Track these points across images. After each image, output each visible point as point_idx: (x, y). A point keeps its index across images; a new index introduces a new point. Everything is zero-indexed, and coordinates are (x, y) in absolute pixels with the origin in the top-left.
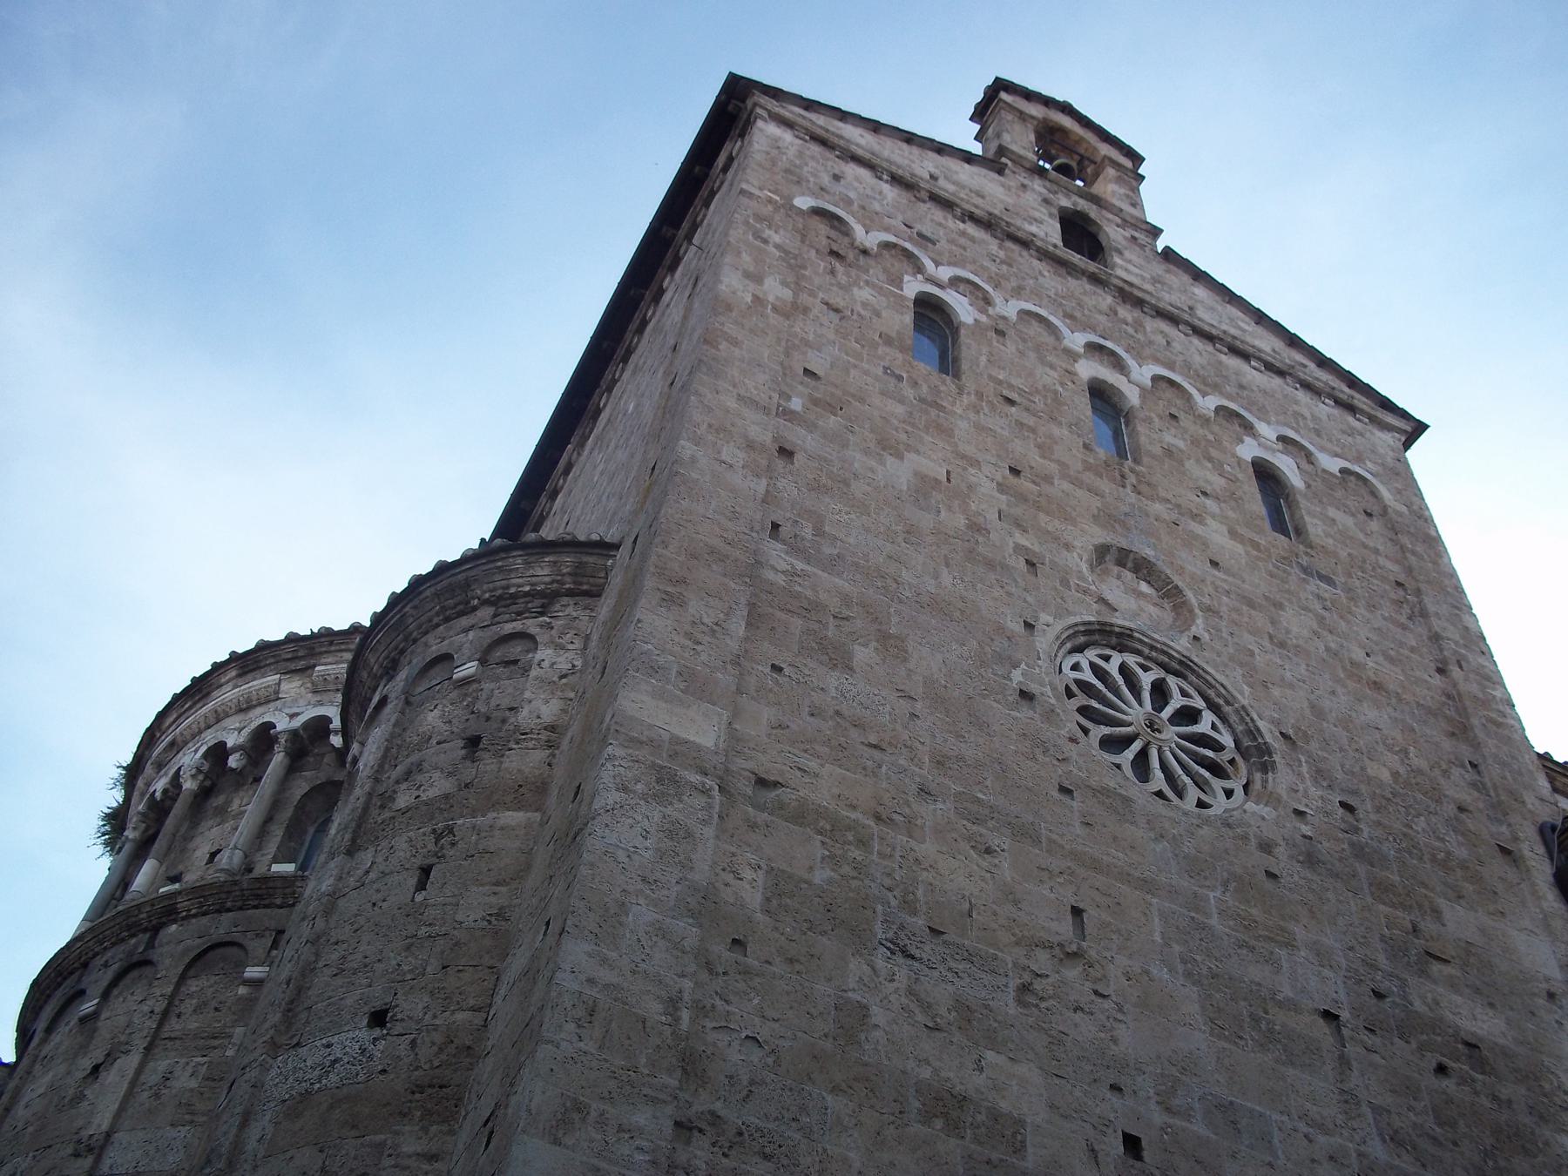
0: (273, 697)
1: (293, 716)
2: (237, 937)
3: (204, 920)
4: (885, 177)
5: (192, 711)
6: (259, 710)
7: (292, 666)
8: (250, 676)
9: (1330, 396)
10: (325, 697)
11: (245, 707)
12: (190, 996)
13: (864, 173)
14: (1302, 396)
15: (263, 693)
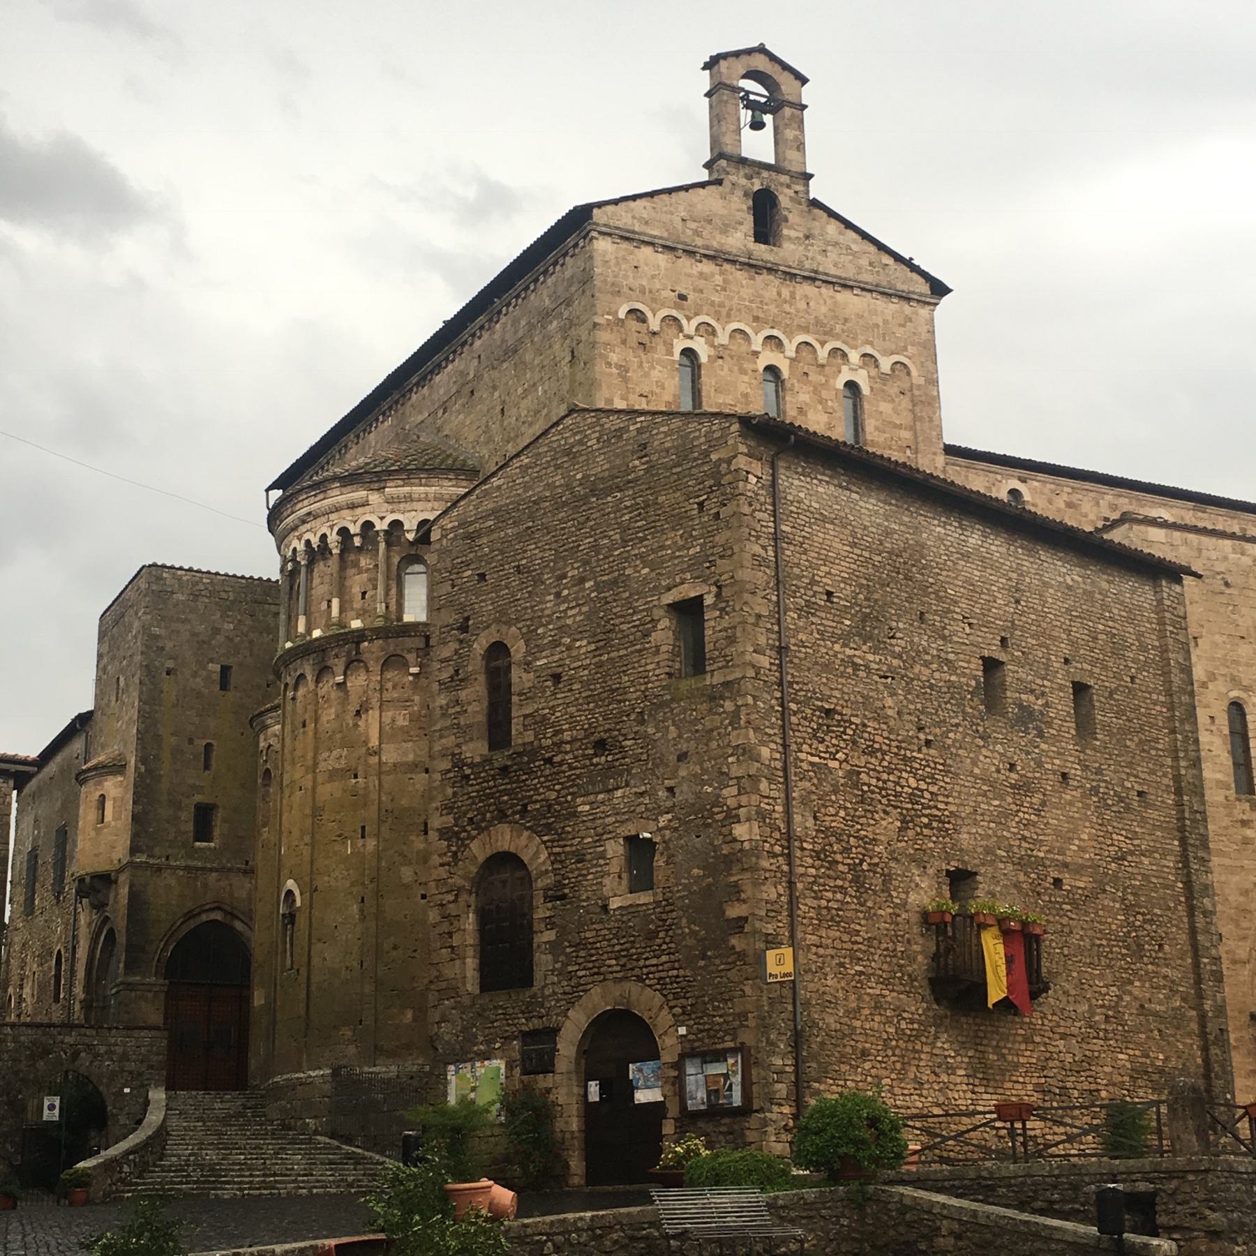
0: (365, 504)
1: (382, 518)
2: (399, 652)
3: (381, 641)
4: (660, 250)
5: (317, 499)
6: (359, 511)
7: (372, 486)
8: (349, 488)
9: (896, 296)
10: (395, 506)
11: (352, 506)
12: (389, 680)
13: (647, 250)
14: (880, 303)
15: (359, 501)
